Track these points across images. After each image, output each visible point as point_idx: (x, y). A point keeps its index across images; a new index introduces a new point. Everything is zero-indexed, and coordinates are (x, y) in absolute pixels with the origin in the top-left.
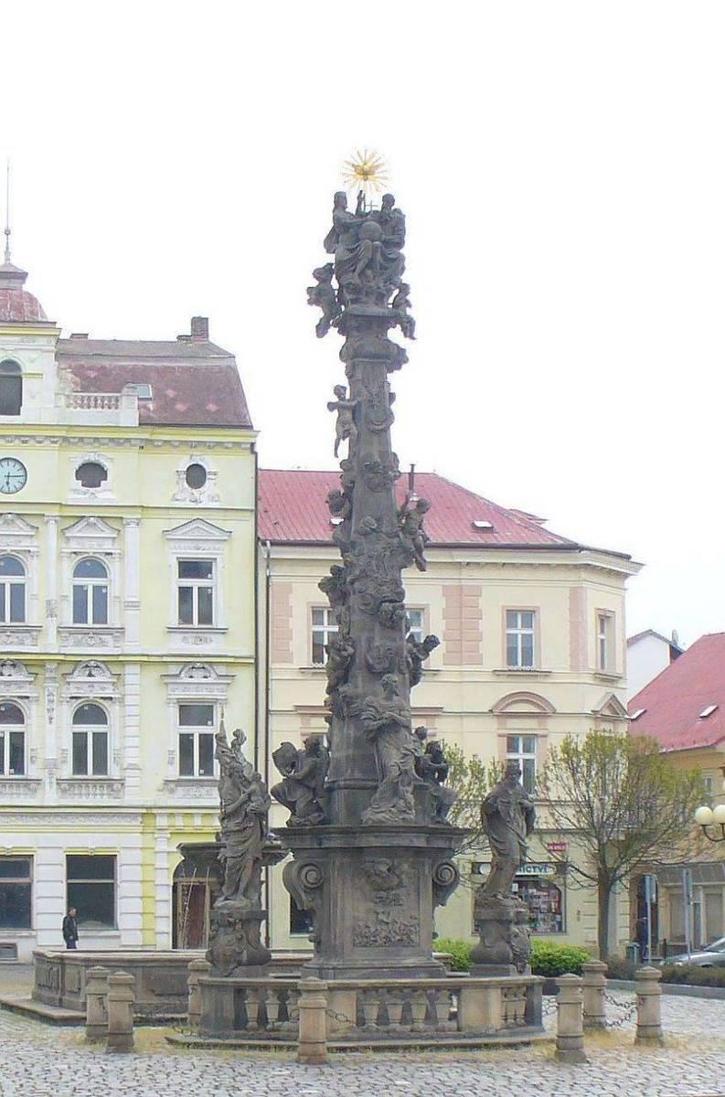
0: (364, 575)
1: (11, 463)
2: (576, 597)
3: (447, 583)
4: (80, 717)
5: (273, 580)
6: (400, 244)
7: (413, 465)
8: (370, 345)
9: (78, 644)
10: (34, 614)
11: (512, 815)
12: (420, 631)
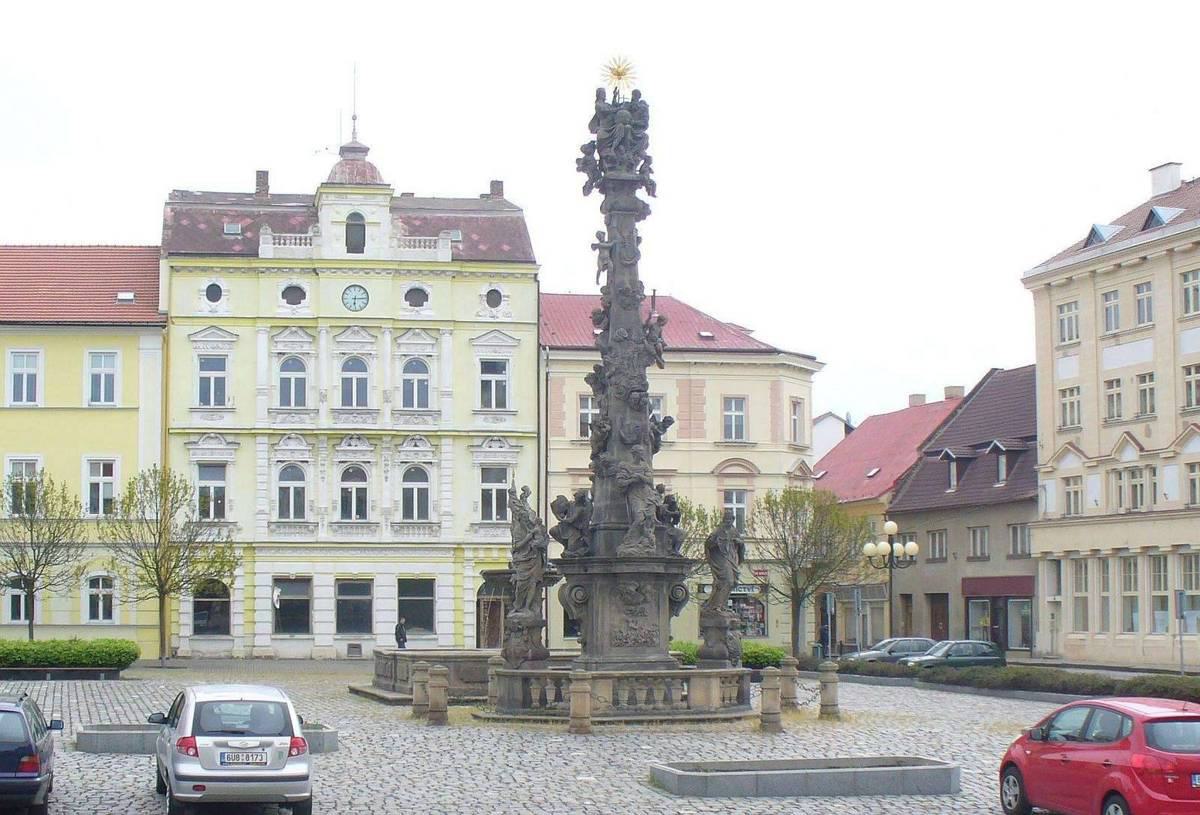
0: (618, 372)
1: (357, 289)
2: (775, 389)
3: (678, 377)
4: (407, 477)
5: (551, 375)
6: (645, 126)
7: (654, 291)
8: (622, 200)
9: (406, 422)
10: (374, 400)
12: (660, 413)
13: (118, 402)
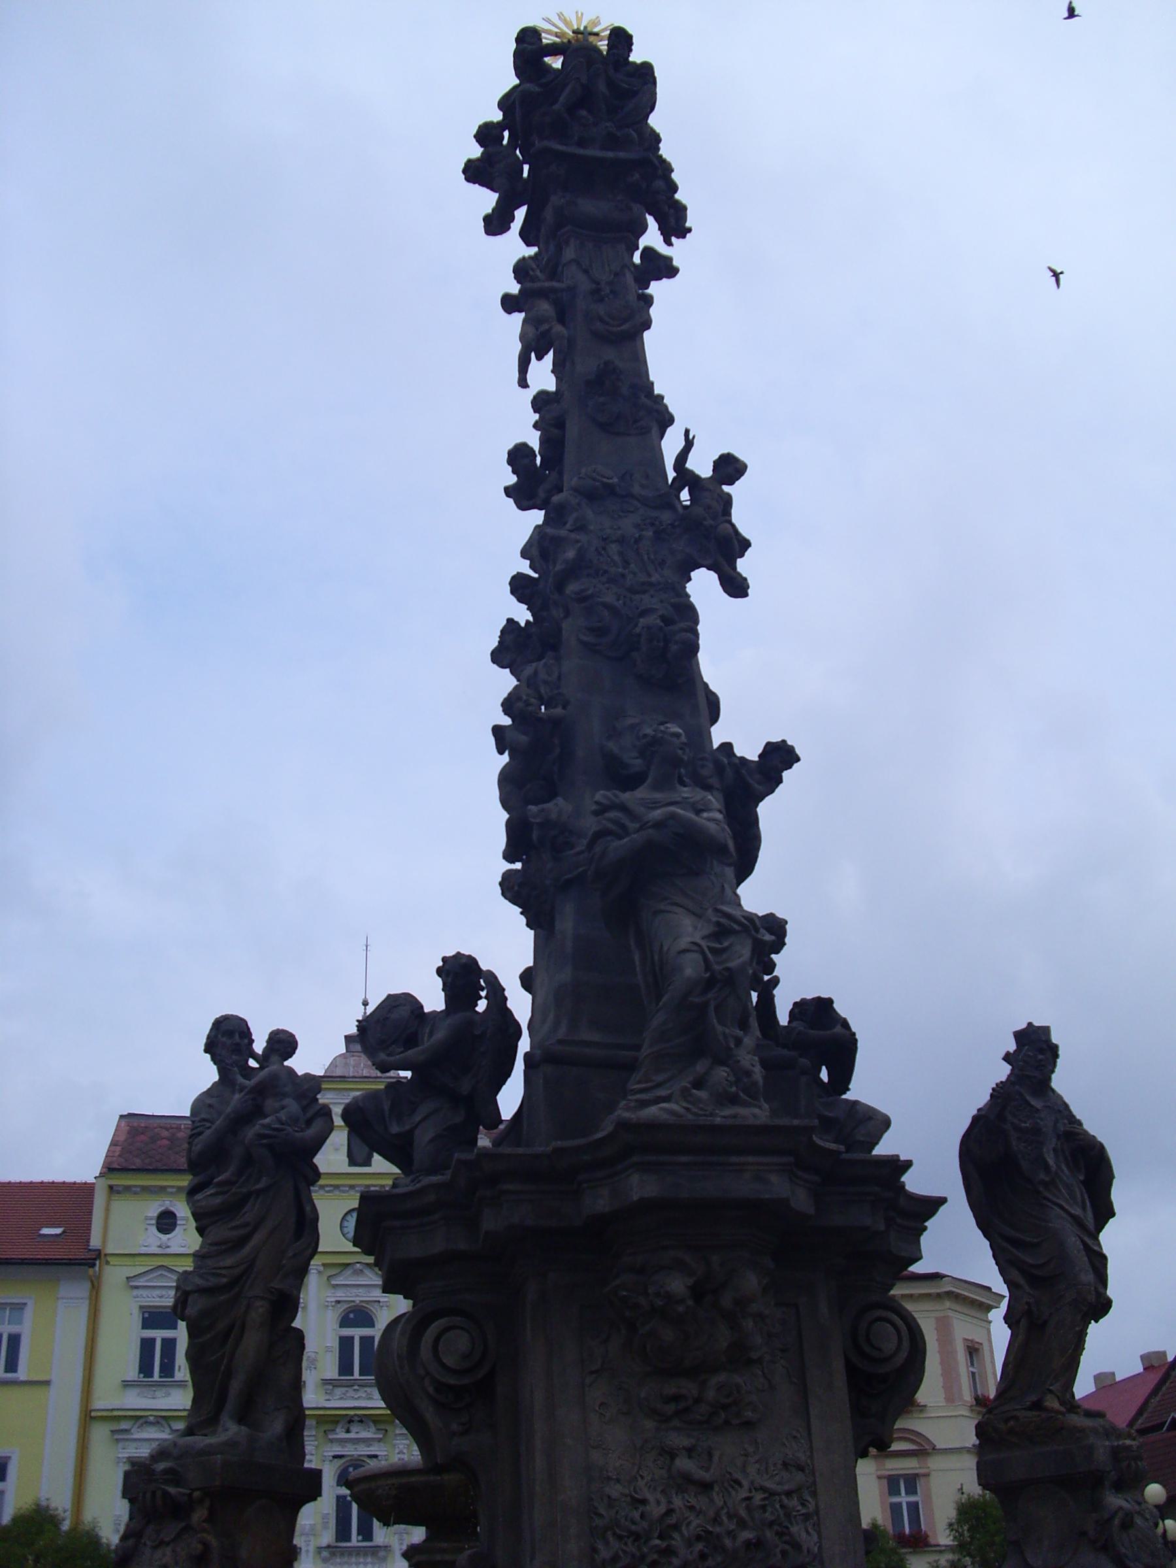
11: (1051, 1162)
13: (22, 1374)
